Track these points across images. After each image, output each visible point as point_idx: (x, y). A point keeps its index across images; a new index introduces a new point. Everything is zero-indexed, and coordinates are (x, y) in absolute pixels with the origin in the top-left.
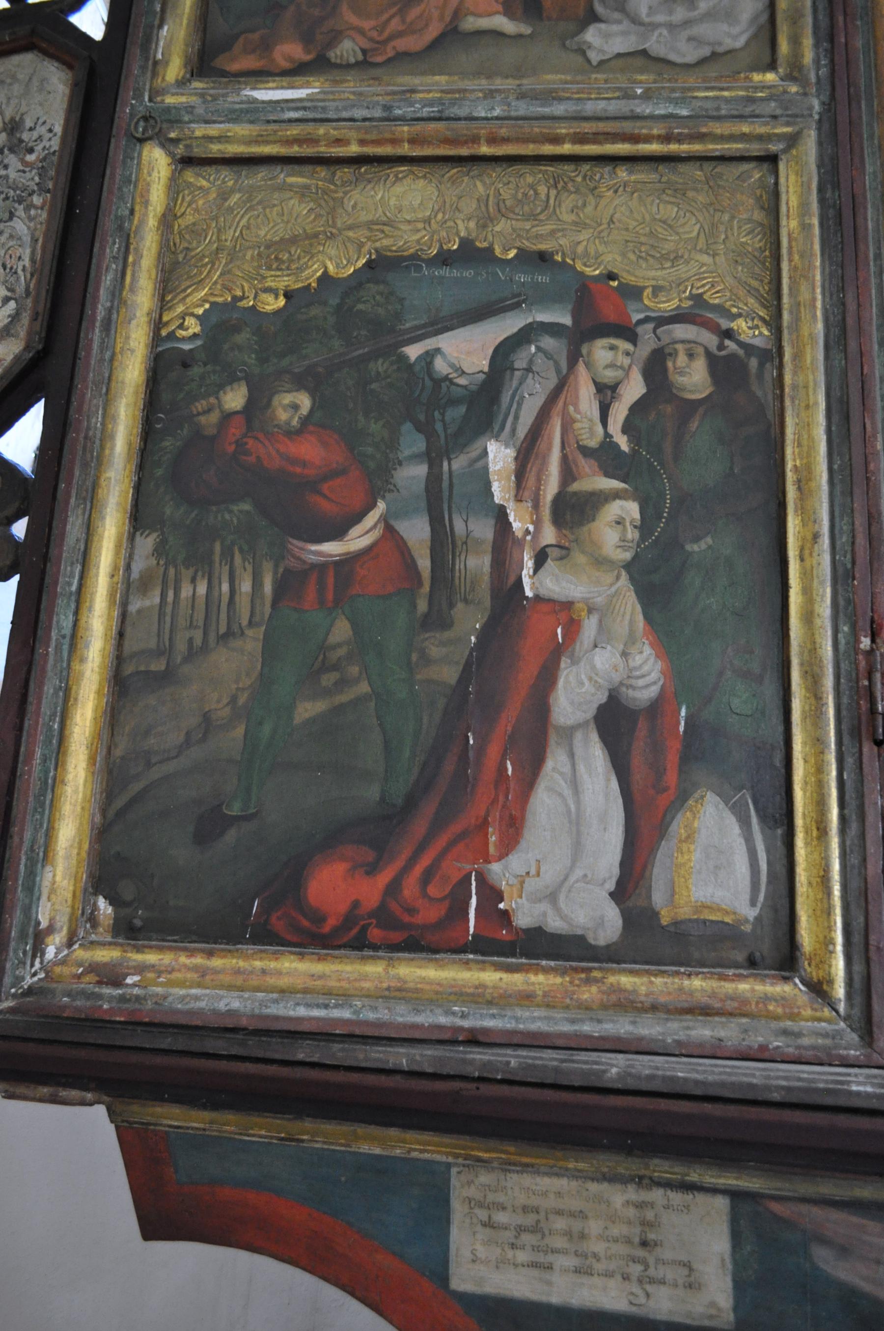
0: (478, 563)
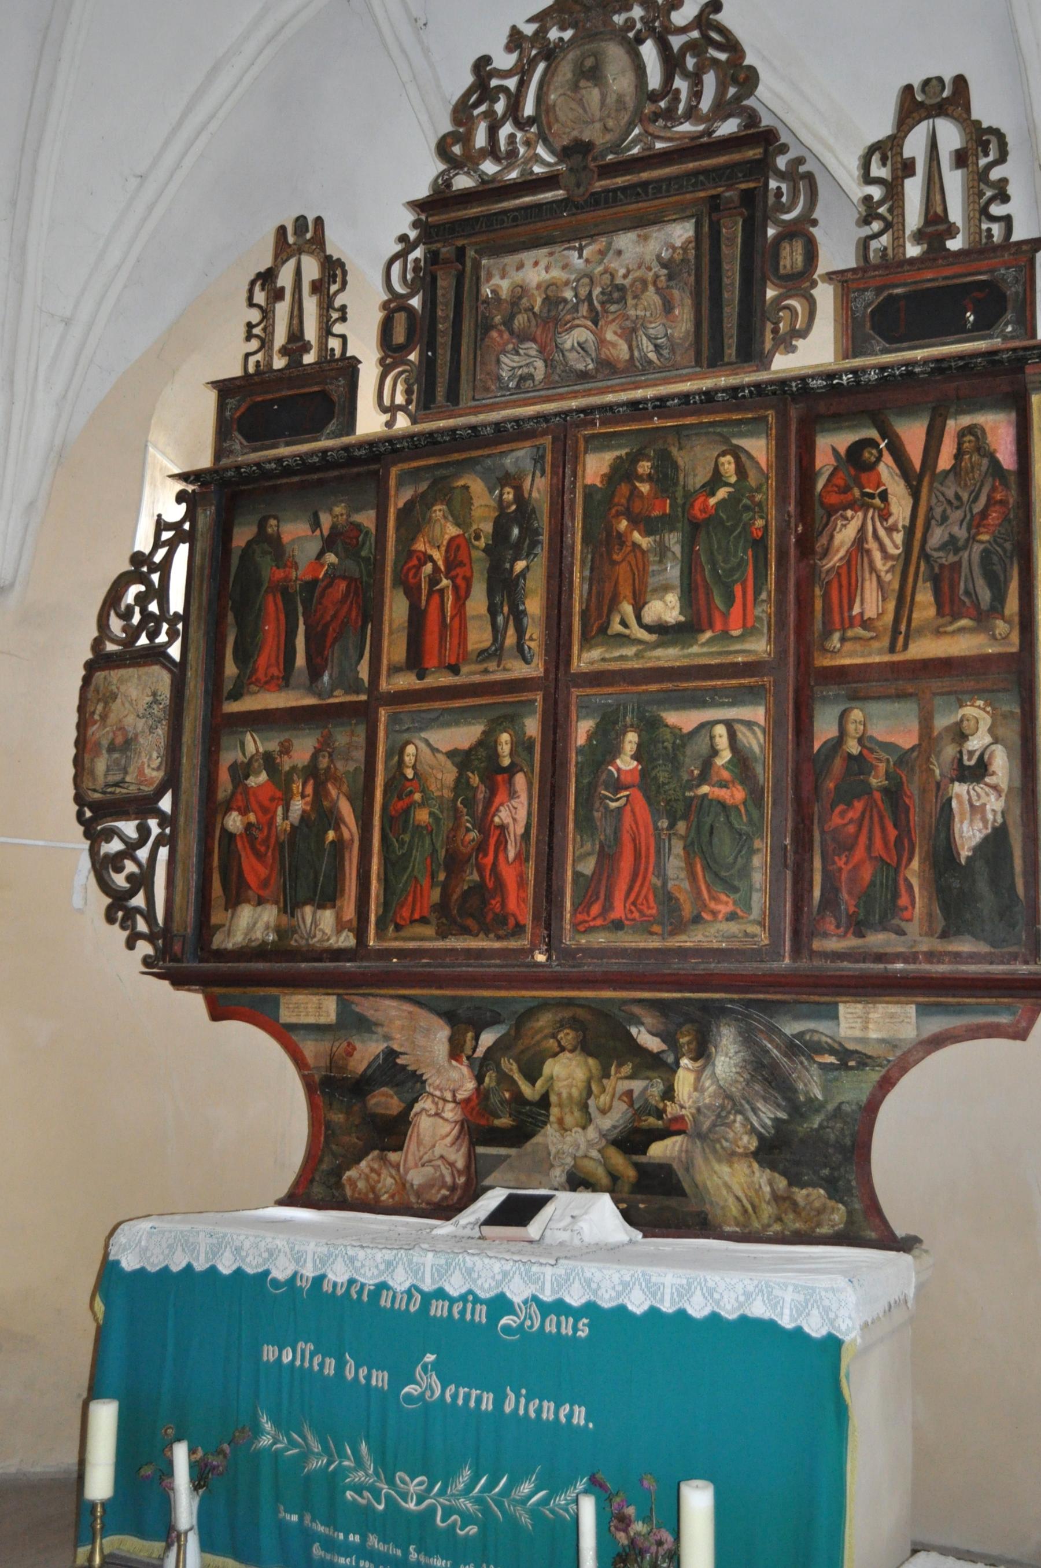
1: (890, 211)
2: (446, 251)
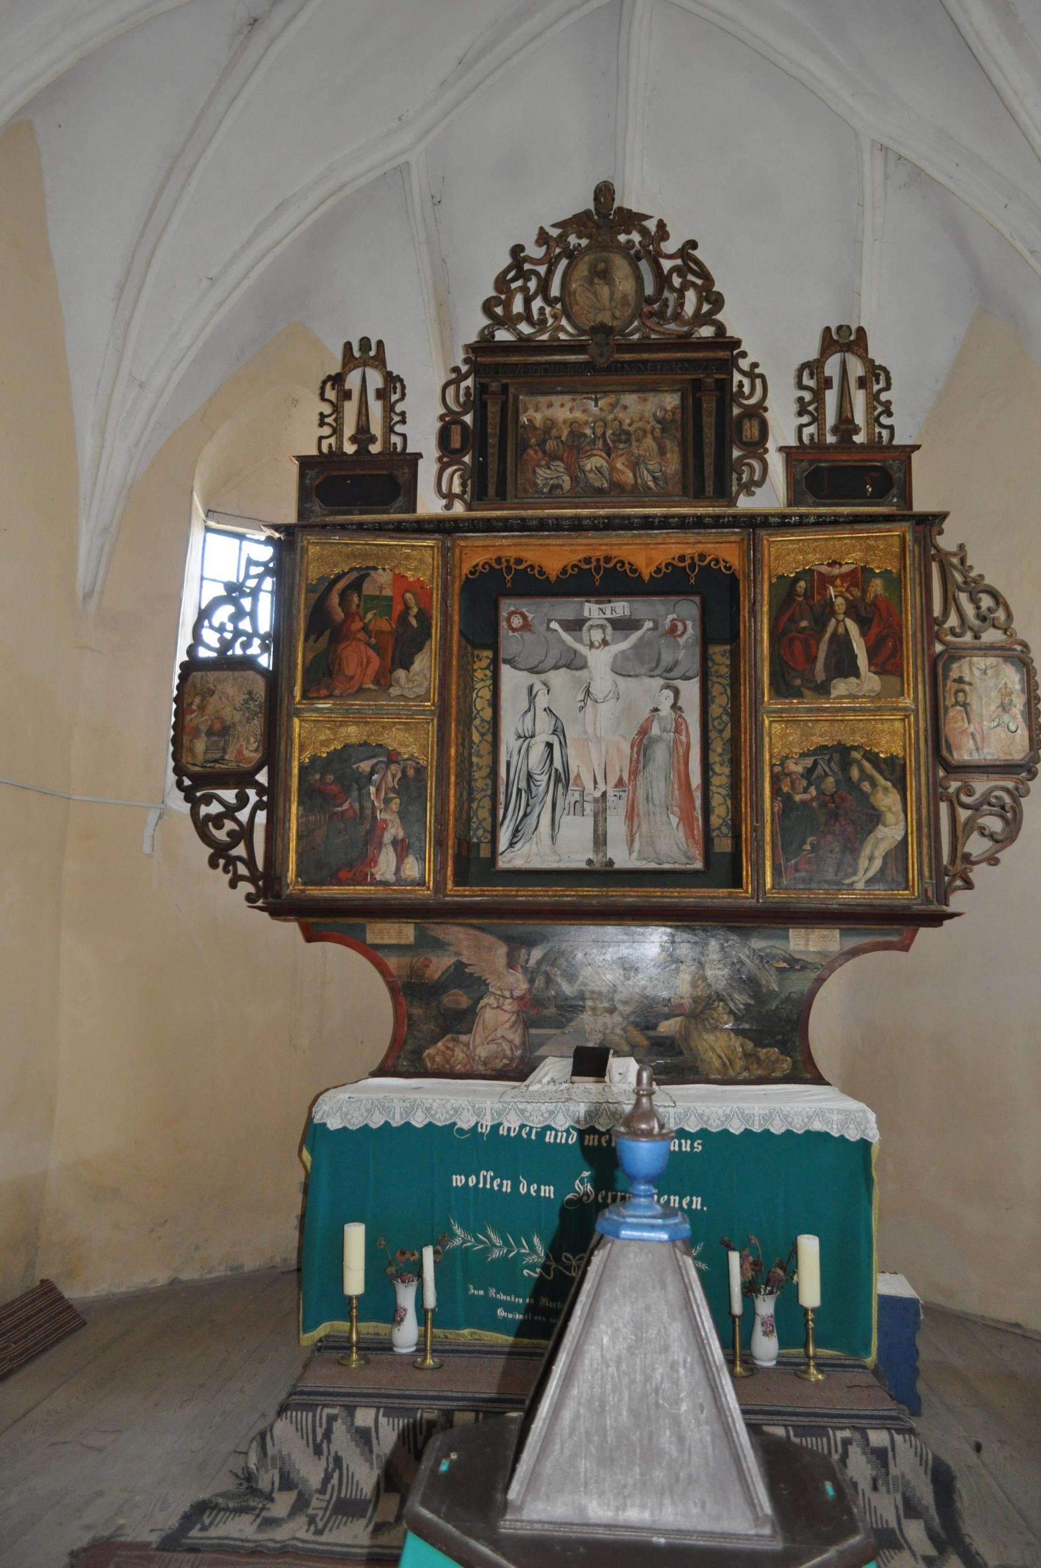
0: (368, 812)
1: (816, 409)
2: (494, 386)
